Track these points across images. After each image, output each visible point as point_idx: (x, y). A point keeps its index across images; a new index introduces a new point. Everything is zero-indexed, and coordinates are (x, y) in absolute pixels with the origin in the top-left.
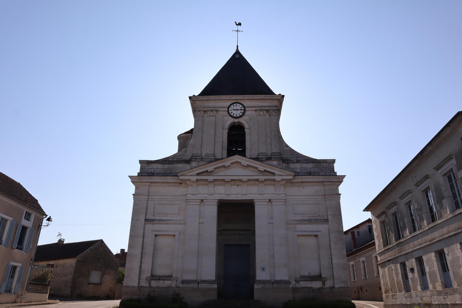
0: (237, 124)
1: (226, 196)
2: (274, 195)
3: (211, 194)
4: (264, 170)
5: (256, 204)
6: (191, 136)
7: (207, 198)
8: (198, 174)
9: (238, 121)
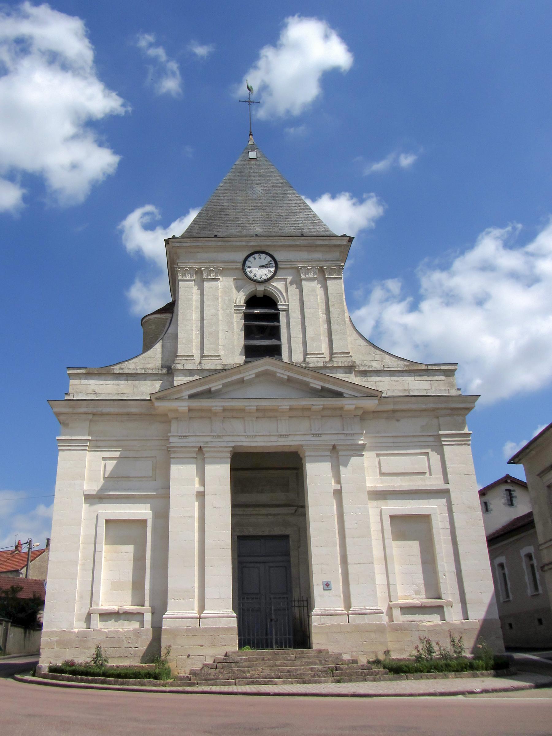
0: (260, 295)
1: (247, 440)
2: (342, 437)
3: (219, 436)
4: (322, 387)
5: (307, 454)
6: (170, 319)
7: (209, 445)
8: (191, 397)
9: (264, 289)
